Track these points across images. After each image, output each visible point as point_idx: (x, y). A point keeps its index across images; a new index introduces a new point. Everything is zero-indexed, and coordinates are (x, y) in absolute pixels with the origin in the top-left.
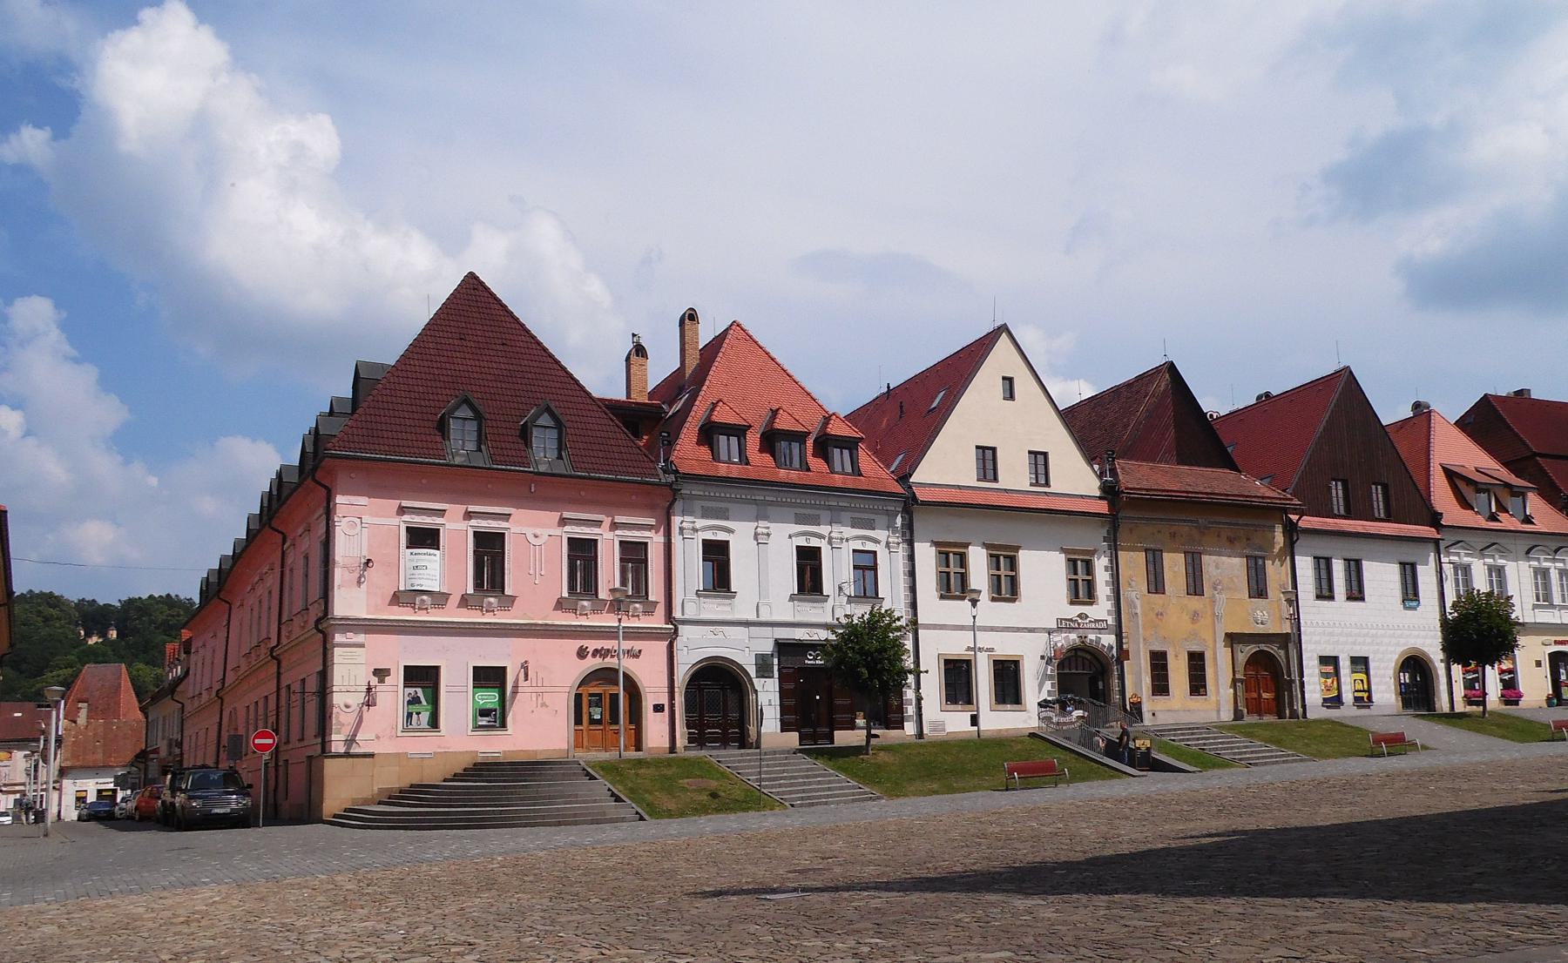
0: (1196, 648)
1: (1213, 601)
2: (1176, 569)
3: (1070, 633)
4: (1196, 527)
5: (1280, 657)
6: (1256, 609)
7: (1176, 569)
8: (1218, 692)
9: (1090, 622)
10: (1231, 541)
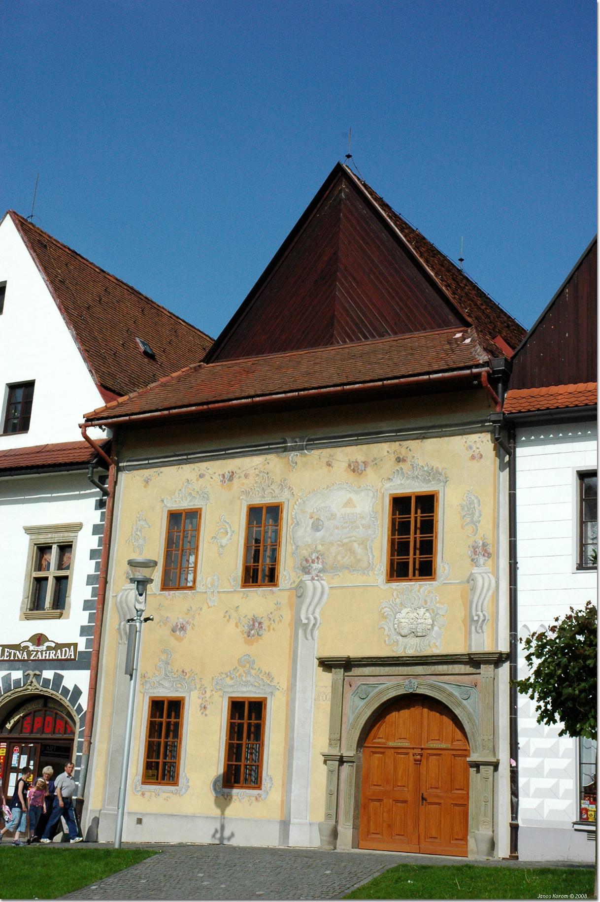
1: (299, 592)
7: (224, 541)
9: (49, 648)
10: (355, 469)
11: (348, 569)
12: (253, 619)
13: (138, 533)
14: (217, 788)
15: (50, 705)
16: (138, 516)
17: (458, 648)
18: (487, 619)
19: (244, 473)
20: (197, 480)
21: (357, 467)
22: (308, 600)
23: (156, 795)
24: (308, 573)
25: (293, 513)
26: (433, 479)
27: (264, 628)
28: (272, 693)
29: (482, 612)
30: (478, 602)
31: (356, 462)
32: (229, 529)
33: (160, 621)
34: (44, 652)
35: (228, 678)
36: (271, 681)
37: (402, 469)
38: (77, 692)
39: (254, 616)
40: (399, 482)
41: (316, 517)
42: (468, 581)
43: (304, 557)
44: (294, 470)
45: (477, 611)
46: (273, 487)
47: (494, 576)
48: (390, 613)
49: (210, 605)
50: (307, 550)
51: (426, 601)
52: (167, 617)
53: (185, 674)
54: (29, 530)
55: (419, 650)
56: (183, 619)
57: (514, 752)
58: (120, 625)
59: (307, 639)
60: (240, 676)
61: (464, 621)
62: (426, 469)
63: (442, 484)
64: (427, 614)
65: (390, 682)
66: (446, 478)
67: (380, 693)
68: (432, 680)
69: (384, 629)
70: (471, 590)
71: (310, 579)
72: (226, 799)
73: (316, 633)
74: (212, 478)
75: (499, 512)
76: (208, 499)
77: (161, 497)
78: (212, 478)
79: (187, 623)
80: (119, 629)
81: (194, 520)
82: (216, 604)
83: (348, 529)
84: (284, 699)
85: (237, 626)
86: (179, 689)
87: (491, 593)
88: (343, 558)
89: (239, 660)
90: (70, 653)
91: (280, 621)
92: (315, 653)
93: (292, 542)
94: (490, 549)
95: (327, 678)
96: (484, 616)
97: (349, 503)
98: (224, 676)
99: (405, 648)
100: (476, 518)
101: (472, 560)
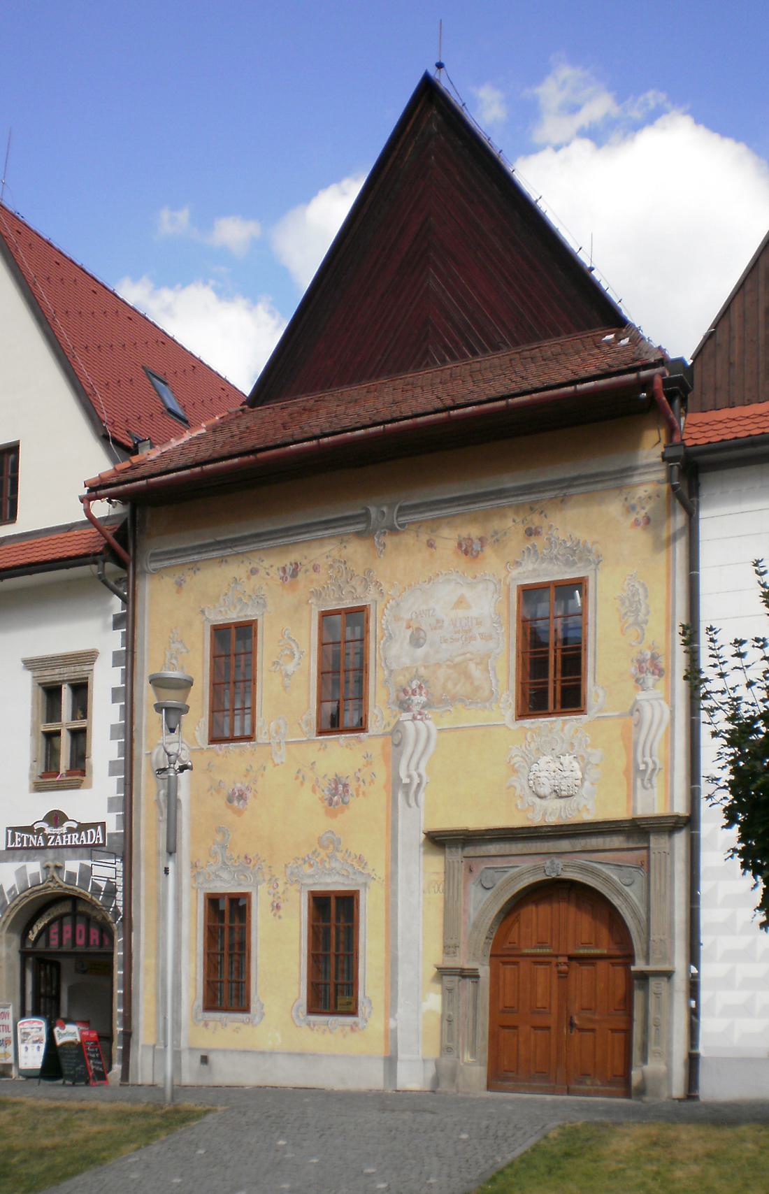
0: (333, 883)
1: (396, 739)
2: (290, 667)
3: (28, 859)
4: (359, 534)
5: (626, 899)
6: (540, 752)
7: (290, 667)
8: (391, 1007)
9: (70, 830)
10: (467, 550)
11: (462, 701)
12: (335, 780)
13: (174, 661)
14: (300, 1014)
15: (81, 908)
16: (171, 635)
17: (618, 811)
18: (658, 767)
19: (312, 564)
20: (249, 578)
21: (471, 546)
22: (408, 749)
23: (222, 1025)
24: (408, 709)
25: (383, 622)
26: (580, 559)
27: (350, 792)
28: (365, 885)
29: (651, 756)
30: (645, 743)
31: (469, 539)
32: (295, 649)
33: (211, 787)
34: (64, 836)
35: (307, 865)
36: (363, 868)
37: (534, 546)
38: (111, 892)
39: (336, 776)
40: (530, 567)
41: (415, 625)
42: (631, 713)
43: (401, 686)
44: (382, 556)
45: (644, 756)
46: (353, 583)
47: (667, 703)
48: (522, 764)
49: (276, 762)
50: (404, 676)
51: (572, 745)
52: (221, 781)
53: (249, 861)
54: (30, 664)
55: (564, 817)
56: (242, 783)
57: (694, 956)
58: (158, 794)
59: (409, 805)
60: (322, 861)
61: (626, 772)
62: (569, 544)
63: (593, 566)
64: (576, 765)
65: (526, 864)
66: (598, 556)
67: (513, 879)
68: (582, 860)
69: (515, 788)
70: (636, 725)
71: (410, 718)
72: (312, 1030)
73: (422, 796)
74: (268, 574)
75: (674, 607)
76: (265, 606)
77: (200, 607)
78: (268, 574)
79: (248, 788)
80: (157, 801)
81: (248, 642)
82: (283, 760)
83: (460, 642)
84: (382, 893)
85: (314, 791)
86: (243, 882)
87: (662, 730)
88: (456, 684)
89: (320, 839)
90: (96, 836)
91: (372, 781)
92: (422, 825)
93: (383, 665)
94: (662, 663)
95: (436, 863)
96: (654, 763)
97: (461, 602)
98: (300, 862)
99: (545, 814)
100: (641, 617)
101: (637, 681)
